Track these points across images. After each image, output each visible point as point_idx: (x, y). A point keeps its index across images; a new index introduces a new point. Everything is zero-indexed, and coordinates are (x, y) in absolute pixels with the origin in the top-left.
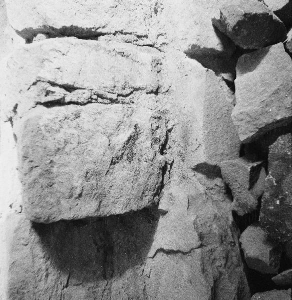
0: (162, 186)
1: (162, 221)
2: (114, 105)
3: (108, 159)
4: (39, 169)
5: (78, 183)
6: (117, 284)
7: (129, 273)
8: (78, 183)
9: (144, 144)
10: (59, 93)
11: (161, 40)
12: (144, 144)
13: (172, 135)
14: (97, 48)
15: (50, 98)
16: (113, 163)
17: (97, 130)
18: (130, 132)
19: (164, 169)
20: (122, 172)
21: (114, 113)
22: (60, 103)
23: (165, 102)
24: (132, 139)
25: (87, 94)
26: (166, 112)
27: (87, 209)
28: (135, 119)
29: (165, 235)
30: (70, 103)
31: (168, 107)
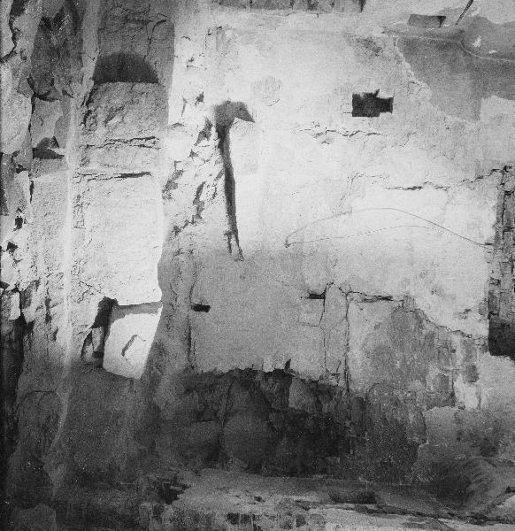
0: (91, 94)
1: (91, 76)
2: (117, 138)
3: (125, 110)
4: (160, 105)
5: (143, 100)
6: (117, 49)
7: (110, 53)
8: (143, 100)
9: (101, 117)
10: (148, 143)
11: (79, 179)
12: (101, 117)
13: (82, 120)
14: (125, 168)
15: (153, 140)
16: (122, 108)
17: (127, 127)
18: (110, 123)
19: (89, 102)
20: (117, 102)
21: (119, 133)
22: (147, 139)
23: (83, 140)
24: (110, 118)
25: (133, 144)
26: (83, 134)
27: (139, 87)
28: (105, 130)
29: (90, 67)
30: (142, 139)
31: (81, 137)
